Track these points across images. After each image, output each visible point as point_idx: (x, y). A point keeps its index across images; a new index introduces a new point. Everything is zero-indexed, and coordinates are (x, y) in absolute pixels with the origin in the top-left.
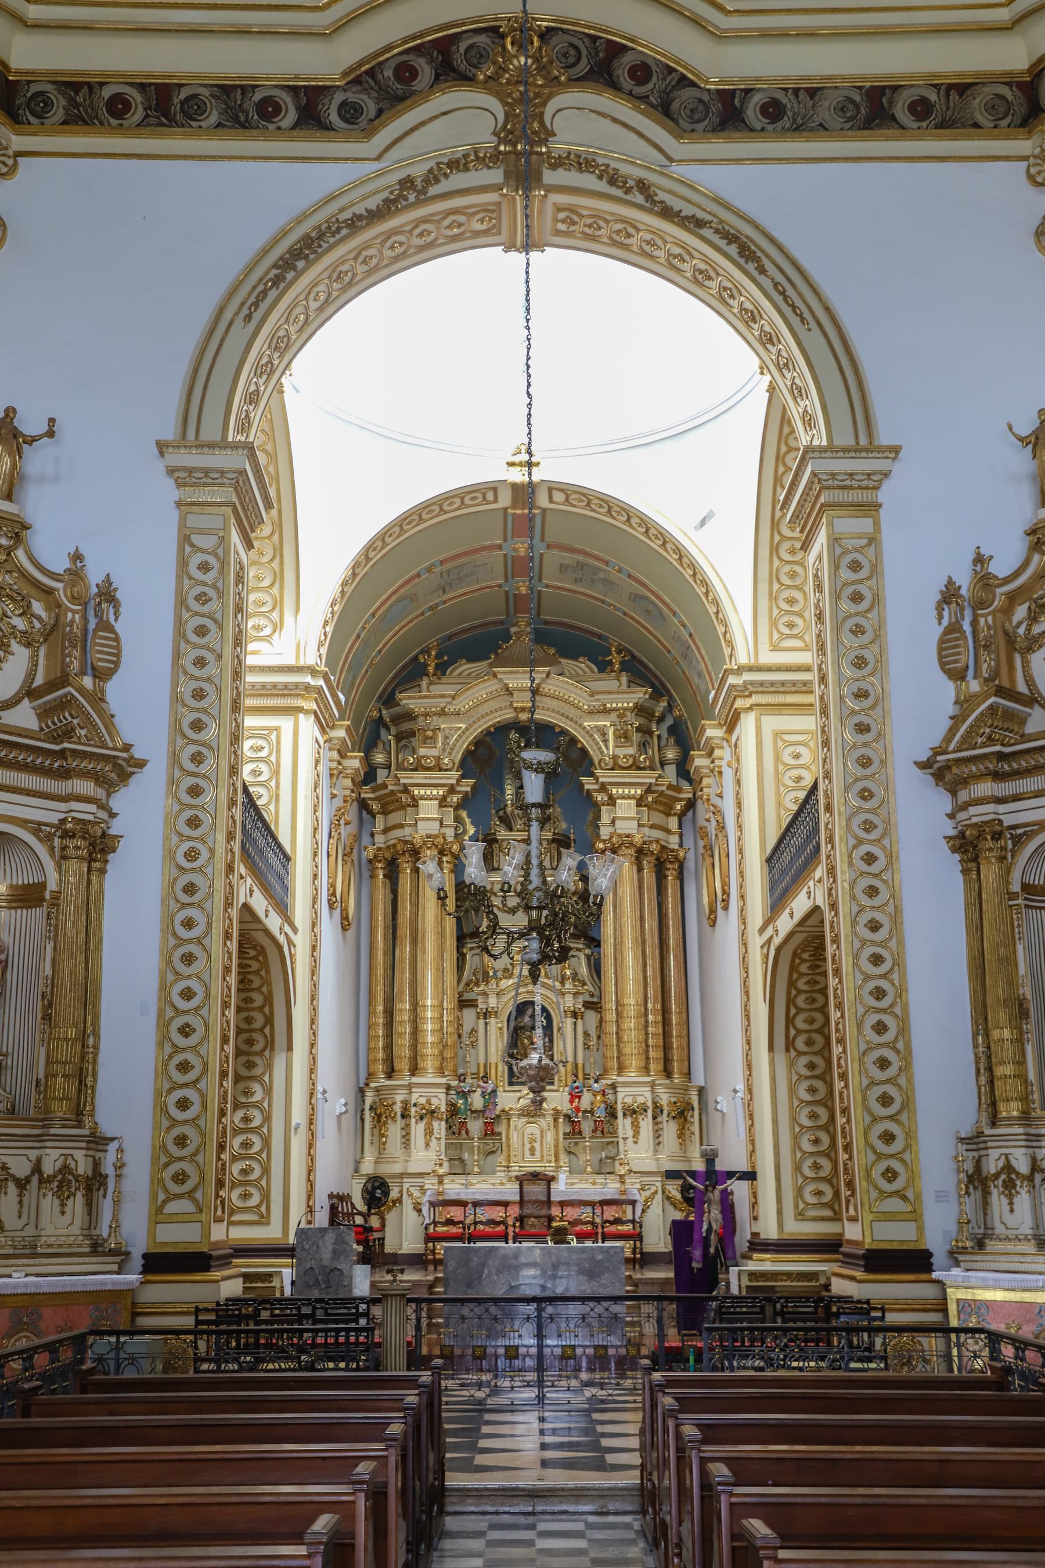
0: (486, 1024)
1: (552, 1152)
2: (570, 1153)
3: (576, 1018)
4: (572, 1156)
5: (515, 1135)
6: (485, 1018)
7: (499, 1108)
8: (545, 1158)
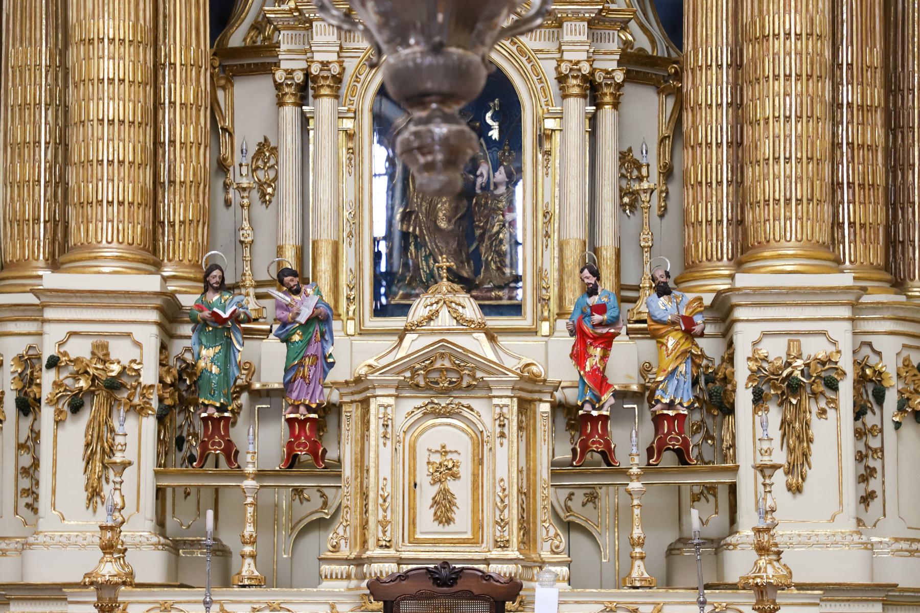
0: (305, 120)
1: (513, 514)
2: (569, 527)
3: (599, 106)
4: (576, 536)
5: (386, 453)
6: (302, 100)
7: (338, 374)
8: (490, 532)
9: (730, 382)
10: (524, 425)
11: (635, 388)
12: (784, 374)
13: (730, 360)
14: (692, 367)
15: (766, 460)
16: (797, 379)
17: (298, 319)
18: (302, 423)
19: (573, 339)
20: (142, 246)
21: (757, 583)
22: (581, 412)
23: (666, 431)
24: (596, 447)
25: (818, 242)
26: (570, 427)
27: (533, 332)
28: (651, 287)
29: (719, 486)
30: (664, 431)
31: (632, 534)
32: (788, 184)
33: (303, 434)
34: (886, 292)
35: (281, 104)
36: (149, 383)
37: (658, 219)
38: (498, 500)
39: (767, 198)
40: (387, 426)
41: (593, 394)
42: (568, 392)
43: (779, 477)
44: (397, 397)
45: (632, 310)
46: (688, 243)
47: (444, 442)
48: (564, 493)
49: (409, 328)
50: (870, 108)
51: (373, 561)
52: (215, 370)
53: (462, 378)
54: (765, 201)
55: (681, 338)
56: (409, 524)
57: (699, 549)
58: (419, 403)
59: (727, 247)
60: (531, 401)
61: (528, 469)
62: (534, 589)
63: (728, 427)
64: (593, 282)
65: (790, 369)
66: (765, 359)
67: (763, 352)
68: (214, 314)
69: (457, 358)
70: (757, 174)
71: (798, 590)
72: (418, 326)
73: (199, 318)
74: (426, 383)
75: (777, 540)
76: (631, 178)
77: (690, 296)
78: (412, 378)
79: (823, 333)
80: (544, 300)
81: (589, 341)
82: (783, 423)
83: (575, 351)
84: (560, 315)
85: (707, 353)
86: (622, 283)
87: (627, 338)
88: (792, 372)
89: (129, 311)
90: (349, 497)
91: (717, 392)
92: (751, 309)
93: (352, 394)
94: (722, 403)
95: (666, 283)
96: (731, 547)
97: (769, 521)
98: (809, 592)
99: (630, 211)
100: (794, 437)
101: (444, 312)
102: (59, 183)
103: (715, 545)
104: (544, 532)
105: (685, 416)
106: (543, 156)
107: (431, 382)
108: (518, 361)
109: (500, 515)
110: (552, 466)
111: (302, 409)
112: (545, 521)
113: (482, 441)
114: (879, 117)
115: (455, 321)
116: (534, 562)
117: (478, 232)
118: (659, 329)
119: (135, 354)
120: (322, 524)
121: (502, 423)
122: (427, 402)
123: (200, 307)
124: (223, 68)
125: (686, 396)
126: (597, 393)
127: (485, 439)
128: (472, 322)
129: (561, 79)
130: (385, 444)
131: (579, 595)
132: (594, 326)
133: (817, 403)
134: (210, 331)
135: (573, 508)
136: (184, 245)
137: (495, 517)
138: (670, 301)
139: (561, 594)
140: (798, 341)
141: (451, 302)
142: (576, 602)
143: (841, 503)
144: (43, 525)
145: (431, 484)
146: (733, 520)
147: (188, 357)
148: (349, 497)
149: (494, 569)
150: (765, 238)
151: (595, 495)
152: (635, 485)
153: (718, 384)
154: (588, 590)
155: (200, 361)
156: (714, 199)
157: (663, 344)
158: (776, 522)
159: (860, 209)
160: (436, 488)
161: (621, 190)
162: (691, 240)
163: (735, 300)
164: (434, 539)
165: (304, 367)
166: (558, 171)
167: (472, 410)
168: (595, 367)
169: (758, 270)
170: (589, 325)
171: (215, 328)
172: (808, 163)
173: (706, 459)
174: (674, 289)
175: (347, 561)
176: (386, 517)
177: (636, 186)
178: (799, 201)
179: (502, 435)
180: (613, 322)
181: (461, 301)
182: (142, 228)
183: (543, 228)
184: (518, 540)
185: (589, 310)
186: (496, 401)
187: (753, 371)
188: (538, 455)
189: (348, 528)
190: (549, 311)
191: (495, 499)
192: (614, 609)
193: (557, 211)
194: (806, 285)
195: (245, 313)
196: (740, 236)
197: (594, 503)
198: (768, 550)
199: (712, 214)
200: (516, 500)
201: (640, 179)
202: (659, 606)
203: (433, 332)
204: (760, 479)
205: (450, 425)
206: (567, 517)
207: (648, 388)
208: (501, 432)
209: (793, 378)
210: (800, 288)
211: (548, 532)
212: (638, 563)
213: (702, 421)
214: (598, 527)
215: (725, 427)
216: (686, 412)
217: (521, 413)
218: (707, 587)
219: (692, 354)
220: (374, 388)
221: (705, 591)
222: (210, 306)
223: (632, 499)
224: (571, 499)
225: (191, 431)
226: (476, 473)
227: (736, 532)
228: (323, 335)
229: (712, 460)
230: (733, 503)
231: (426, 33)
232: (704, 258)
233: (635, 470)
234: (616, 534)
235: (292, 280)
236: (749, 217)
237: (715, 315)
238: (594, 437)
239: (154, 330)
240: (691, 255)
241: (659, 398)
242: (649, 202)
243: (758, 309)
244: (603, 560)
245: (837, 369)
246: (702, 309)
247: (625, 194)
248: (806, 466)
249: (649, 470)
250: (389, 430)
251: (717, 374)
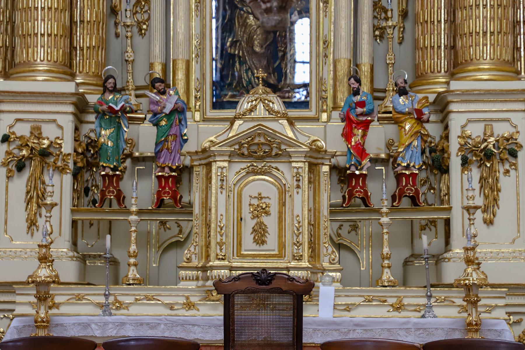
2: (339, 247)
5: (222, 198)
7: (190, 147)
9: (446, 152)
10: (312, 180)
11: (383, 156)
12: (482, 147)
14: (421, 142)
15: (471, 203)
16: (490, 150)
17: (164, 111)
18: (167, 178)
19: (344, 124)
20: (63, 63)
21: (466, 284)
22: (348, 172)
23: (404, 184)
24: (359, 195)
25: (504, 60)
26: (341, 181)
27: (316, 119)
28: (393, 90)
29: (439, 220)
30: (403, 184)
31: (383, 251)
32: (485, 22)
33: (167, 186)
36: (67, 152)
37: (398, 45)
38: (295, 229)
39: (471, 31)
40: (223, 180)
41: (357, 160)
42: (339, 158)
43: (479, 215)
44: (230, 162)
45: (381, 105)
46: (419, 61)
47: (260, 191)
48: (336, 225)
49: (238, 117)
51: (214, 268)
52: (110, 144)
53: (272, 149)
54: (470, 33)
55: (414, 123)
56: (237, 245)
57: (427, 261)
58: (244, 165)
59: (444, 63)
60: (316, 165)
61: (315, 209)
62: (319, 287)
63: (445, 182)
64: (357, 87)
65: (486, 144)
66: (469, 137)
68: (110, 107)
69: (269, 137)
70: (465, 15)
71: (491, 288)
72: (243, 115)
73: (100, 110)
74: (249, 153)
75: (477, 255)
76: (381, 18)
77: (420, 96)
78: (239, 149)
79: (508, 120)
80: (323, 98)
81: (354, 125)
82: (481, 179)
83: (344, 132)
84: (335, 108)
85: (431, 134)
86: (374, 87)
87: (378, 123)
88: (487, 146)
89: (55, 105)
90: (198, 227)
91: (437, 159)
92: (460, 104)
93: (200, 159)
94: (441, 166)
95: (404, 87)
96: (447, 260)
97: (473, 243)
98: (499, 289)
99: (380, 40)
100: (488, 189)
101: (261, 107)
102: (8, 22)
103: (436, 259)
104: (325, 250)
105: (417, 174)
106: (323, 4)
107: (252, 152)
108: (308, 138)
109: (297, 239)
110: (330, 207)
111: (167, 169)
112: (325, 243)
113: (285, 190)
115: (267, 112)
116: (319, 269)
117: (280, 54)
118: (400, 118)
119: (59, 133)
121: (298, 179)
122: (249, 165)
123: (100, 103)
125: (417, 161)
126: (359, 159)
127: (287, 189)
128: (279, 113)
130: (221, 193)
131: (348, 291)
132: (357, 115)
133: (503, 166)
134: (107, 119)
135: (342, 235)
136: (90, 62)
137: (293, 240)
138: (407, 99)
139: (336, 291)
140: (491, 125)
141: (265, 100)
142: (346, 296)
143: (519, 231)
145: (252, 219)
146: (447, 242)
147: (92, 135)
148: (198, 227)
149: (292, 273)
150: (470, 58)
151: (357, 226)
152: (385, 220)
153: (438, 153)
154: (354, 288)
155: (100, 138)
156: (436, 32)
157: (402, 127)
158: (477, 244)
160: (255, 221)
161: (374, 26)
162: (421, 59)
163: (450, 98)
164: (254, 254)
165: (168, 142)
166: (333, 14)
167: (278, 170)
168: (358, 142)
169: (465, 79)
170: (354, 115)
171: (110, 117)
172: (498, 8)
173: (430, 203)
174: (409, 91)
175: (197, 268)
176: (222, 240)
177: (384, 24)
178: (492, 33)
179: (298, 187)
180: (370, 113)
181: (272, 99)
182: (63, 51)
183: (323, 51)
184: (308, 255)
185: (354, 105)
186: (294, 164)
187: (461, 145)
188: (321, 200)
189: (197, 247)
190: (327, 105)
191: (293, 229)
192: (371, 300)
193: (332, 40)
194: (497, 88)
195: (130, 107)
196: (452, 57)
197: (356, 231)
198: (473, 262)
199: (434, 42)
200: (307, 229)
201: (387, 19)
202: (400, 299)
203: (253, 119)
204: (466, 215)
205: (264, 180)
206: (338, 240)
207: (391, 156)
208: (297, 185)
209: (488, 150)
210: (493, 90)
211: (327, 250)
212: (386, 270)
213: (427, 177)
214: (358, 247)
215: (442, 181)
216: (417, 172)
217: (310, 172)
218: (432, 286)
219: (421, 134)
220: (215, 156)
221: (431, 289)
222: (107, 102)
223: (383, 229)
224: (340, 229)
225: (94, 183)
226: (281, 211)
227: (450, 250)
228: (180, 121)
229: (434, 203)
230: (448, 231)
232: (429, 71)
233: (385, 210)
234: (370, 252)
235: (160, 86)
236: (459, 44)
237: (436, 108)
238: (357, 188)
240: (421, 69)
241: (400, 162)
242: (392, 34)
243: (465, 104)
244: (362, 269)
245: (516, 143)
246: (428, 104)
247: (377, 29)
248: (496, 207)
249: (393, 209)
250: (225, 183)
251: (437, 147)
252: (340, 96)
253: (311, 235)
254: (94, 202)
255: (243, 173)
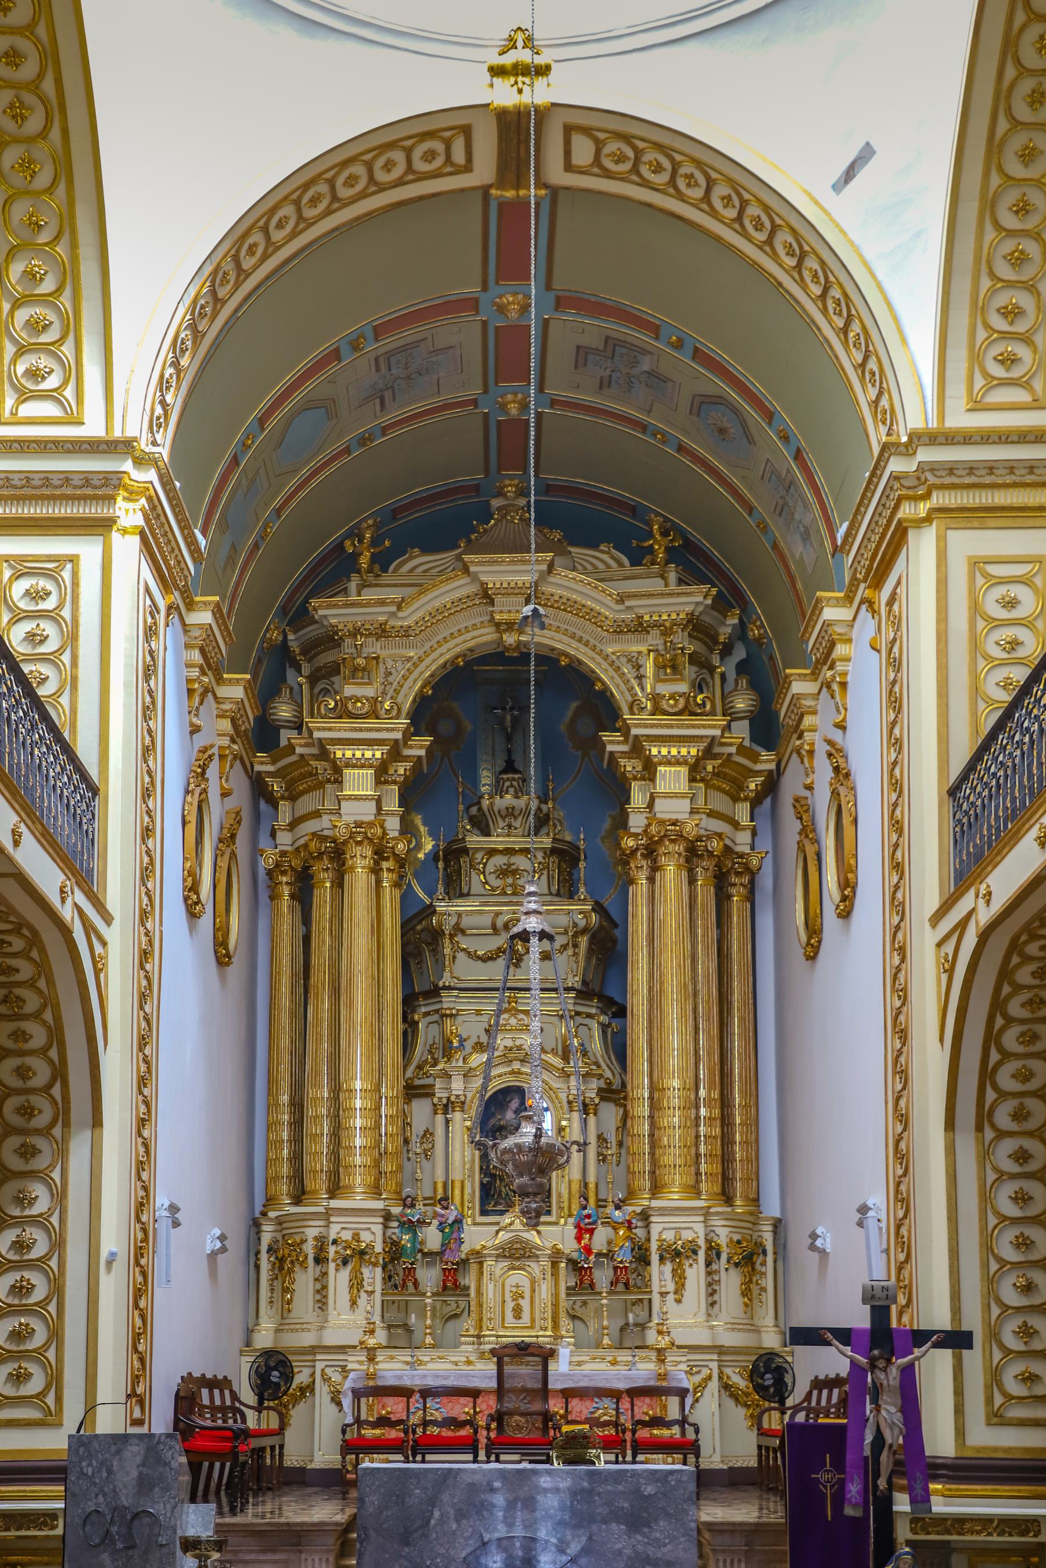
1: (549, 1315)
2: (574, 1317)
3: (587, 1114)
4: (577, 1322)
5: (491, 1287)
7: (465, 1248)
13: (648, 1240)
18: (449, 1270)
34: (721, 1206)
35: (436, 1113)
48: (571, 1302)
50: (715, 1119)
60: (557, 1262)
66: (664, 1240)
67: (664, 1237)
114: (718, 1122)
120: (456, 1316)
123: (402, 1215)
124: (407, 1094)
125: (629, 1258)
129: (570, 1102)
144: (330, 1318)
146: (650, 1316)
147: (394, 1237)
159: (710, 1166)
175: (473, 1336)
203: (512, 1231)
212: (606, 1337)
218: (637, 1348)
231: (530, 1173)
236: (657, 1172)
239: (381, 1226)
252: (573, 1207)
253: (553, 1313)
254: (396, 1286)
255: (506, 1269)
